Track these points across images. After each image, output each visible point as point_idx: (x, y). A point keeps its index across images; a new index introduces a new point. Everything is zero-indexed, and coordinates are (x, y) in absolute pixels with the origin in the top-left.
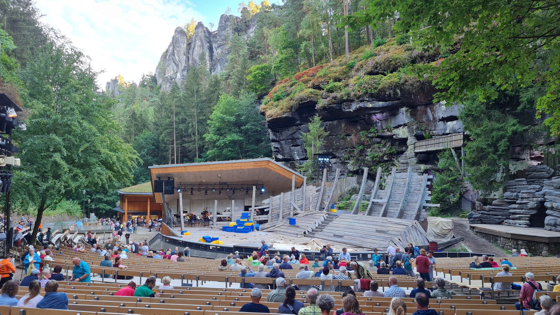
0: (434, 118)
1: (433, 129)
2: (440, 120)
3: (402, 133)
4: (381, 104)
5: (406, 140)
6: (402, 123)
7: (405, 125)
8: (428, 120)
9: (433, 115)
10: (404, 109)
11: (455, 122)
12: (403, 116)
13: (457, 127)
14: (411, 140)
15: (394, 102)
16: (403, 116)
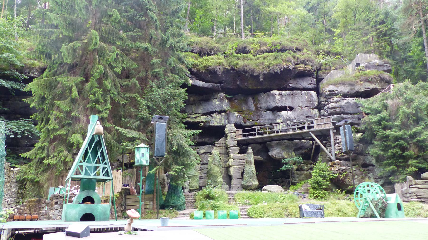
0: (257, 108)
1: (256, 118)
2: (268, 110)
3: (216, 121)
4: (200, 83)
5: (224, 127)
6: (217, 109)
7: (221, 112)
8: (249, 109)
9: (256, 105)
10: (223, 95)
11: (290, 113)
12: (220, 102)
13: (292, 117)
14: (230, 128)
15: (215, 85)
16: (220, 102)
